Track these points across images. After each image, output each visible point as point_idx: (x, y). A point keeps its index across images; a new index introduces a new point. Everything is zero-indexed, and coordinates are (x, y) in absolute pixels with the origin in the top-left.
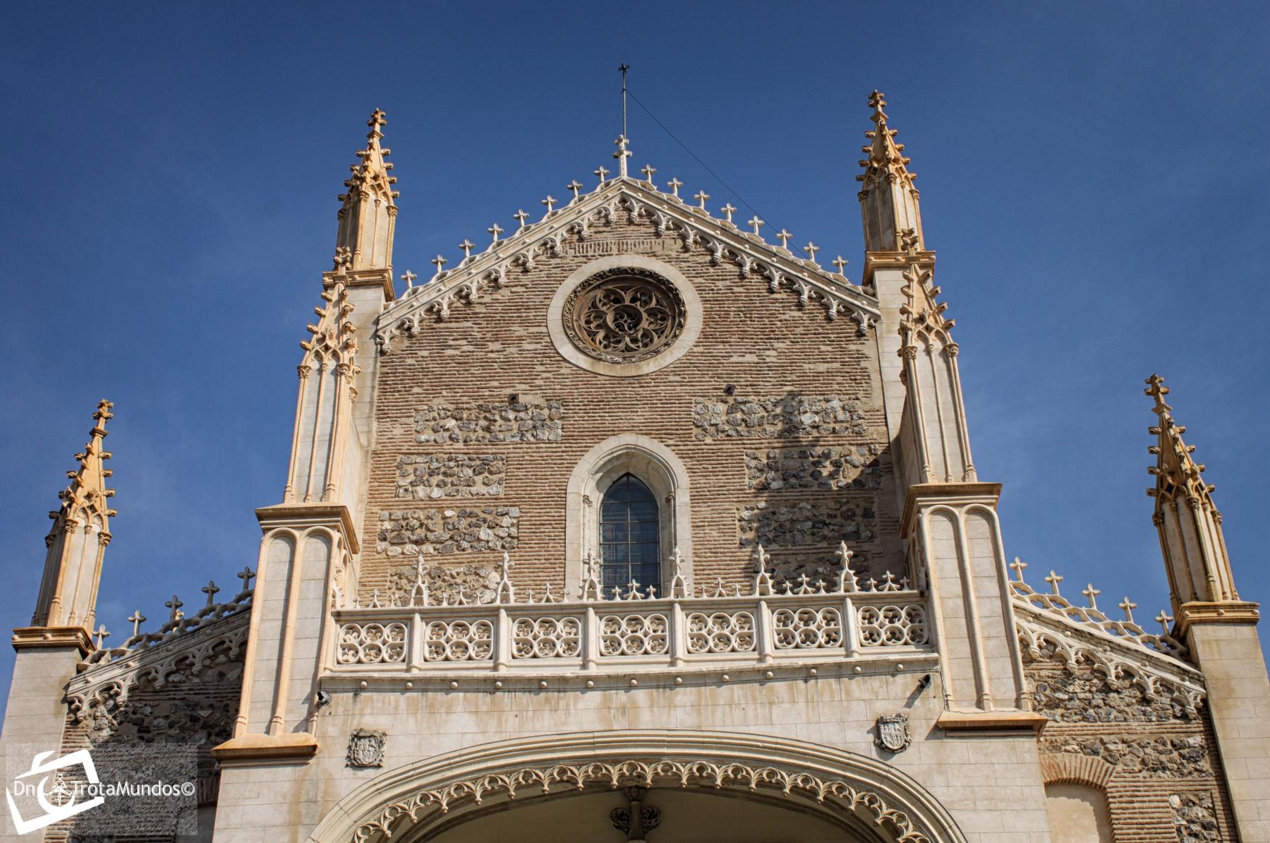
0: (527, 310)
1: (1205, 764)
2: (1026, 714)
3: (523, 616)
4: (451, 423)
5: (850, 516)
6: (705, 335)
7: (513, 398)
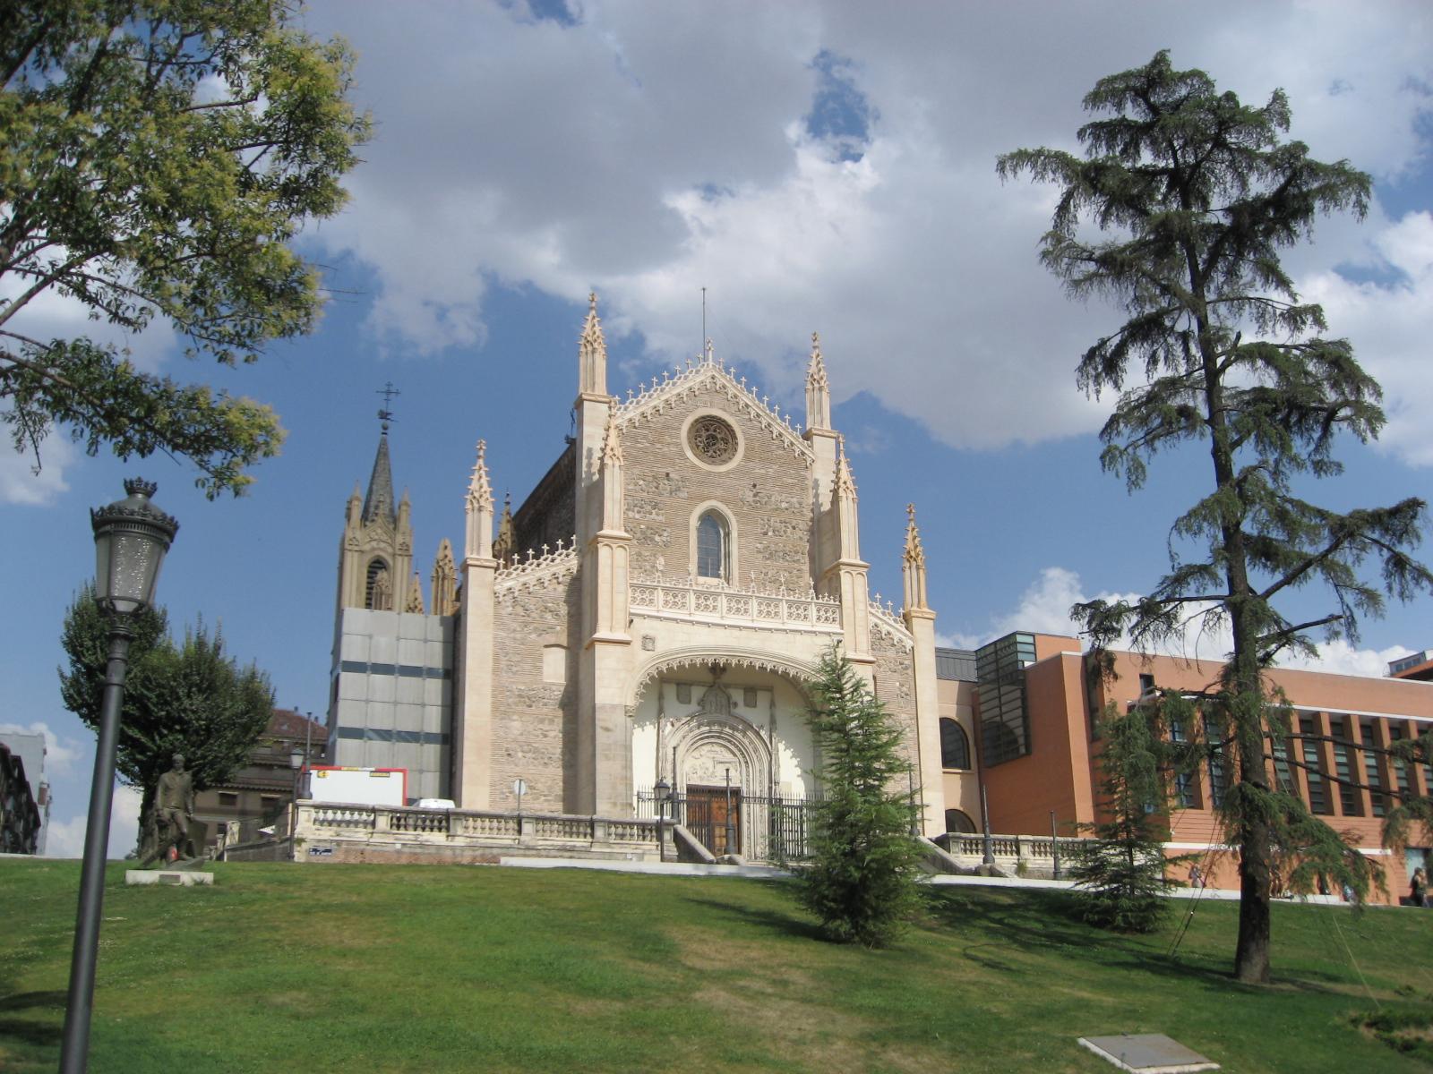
0: (670, 428)
1: (910, 672)
2: (871, 658)
3: (699, 594)
4: (641, 482)
5: (796, 552)
6: (745, 456)
7: (668, 475)
